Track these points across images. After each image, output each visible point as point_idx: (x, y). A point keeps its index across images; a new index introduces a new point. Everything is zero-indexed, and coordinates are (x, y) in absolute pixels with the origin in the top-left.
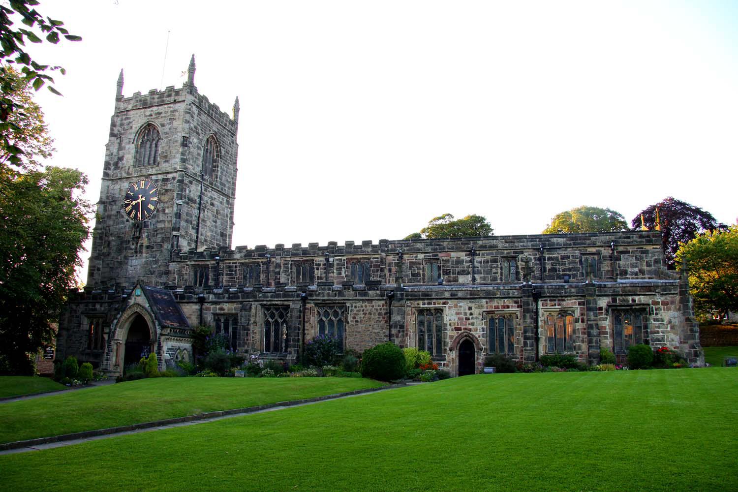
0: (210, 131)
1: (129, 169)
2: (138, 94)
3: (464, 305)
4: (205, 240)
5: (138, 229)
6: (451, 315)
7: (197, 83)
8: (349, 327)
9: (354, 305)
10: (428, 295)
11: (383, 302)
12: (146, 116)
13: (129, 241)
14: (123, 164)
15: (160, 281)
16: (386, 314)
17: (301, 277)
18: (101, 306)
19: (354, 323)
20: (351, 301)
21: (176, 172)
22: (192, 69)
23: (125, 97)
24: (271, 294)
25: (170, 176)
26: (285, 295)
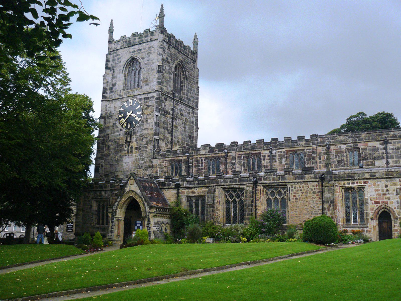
0: (177, 60)
1: (120, 92)
2: (123, 37)
3: (381, 183)
4: (178, 142)
5: (129, 136)
7: (165, 26)
8: (290, 203)
9: (294, 186)
10: (352, 177)
11: (316, 183)
12: (130, 53)
13: (123, 145)
14: (116, 89)
15: (146, 173)
16: (319, 192)
17: (251, 166)
18: (105, 193)
19: (294, 200)
20: (292, 183)
21: (155, 92)
22: (161, 16)
23: (115, 40)
24: (230, 180)
25: (150, 95)
26: (240, 181)
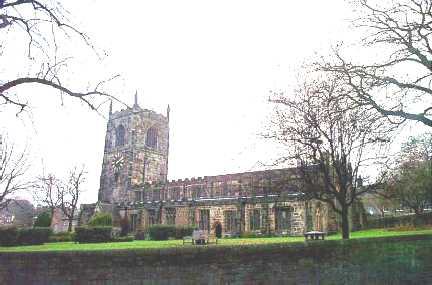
6: (212, 213)
